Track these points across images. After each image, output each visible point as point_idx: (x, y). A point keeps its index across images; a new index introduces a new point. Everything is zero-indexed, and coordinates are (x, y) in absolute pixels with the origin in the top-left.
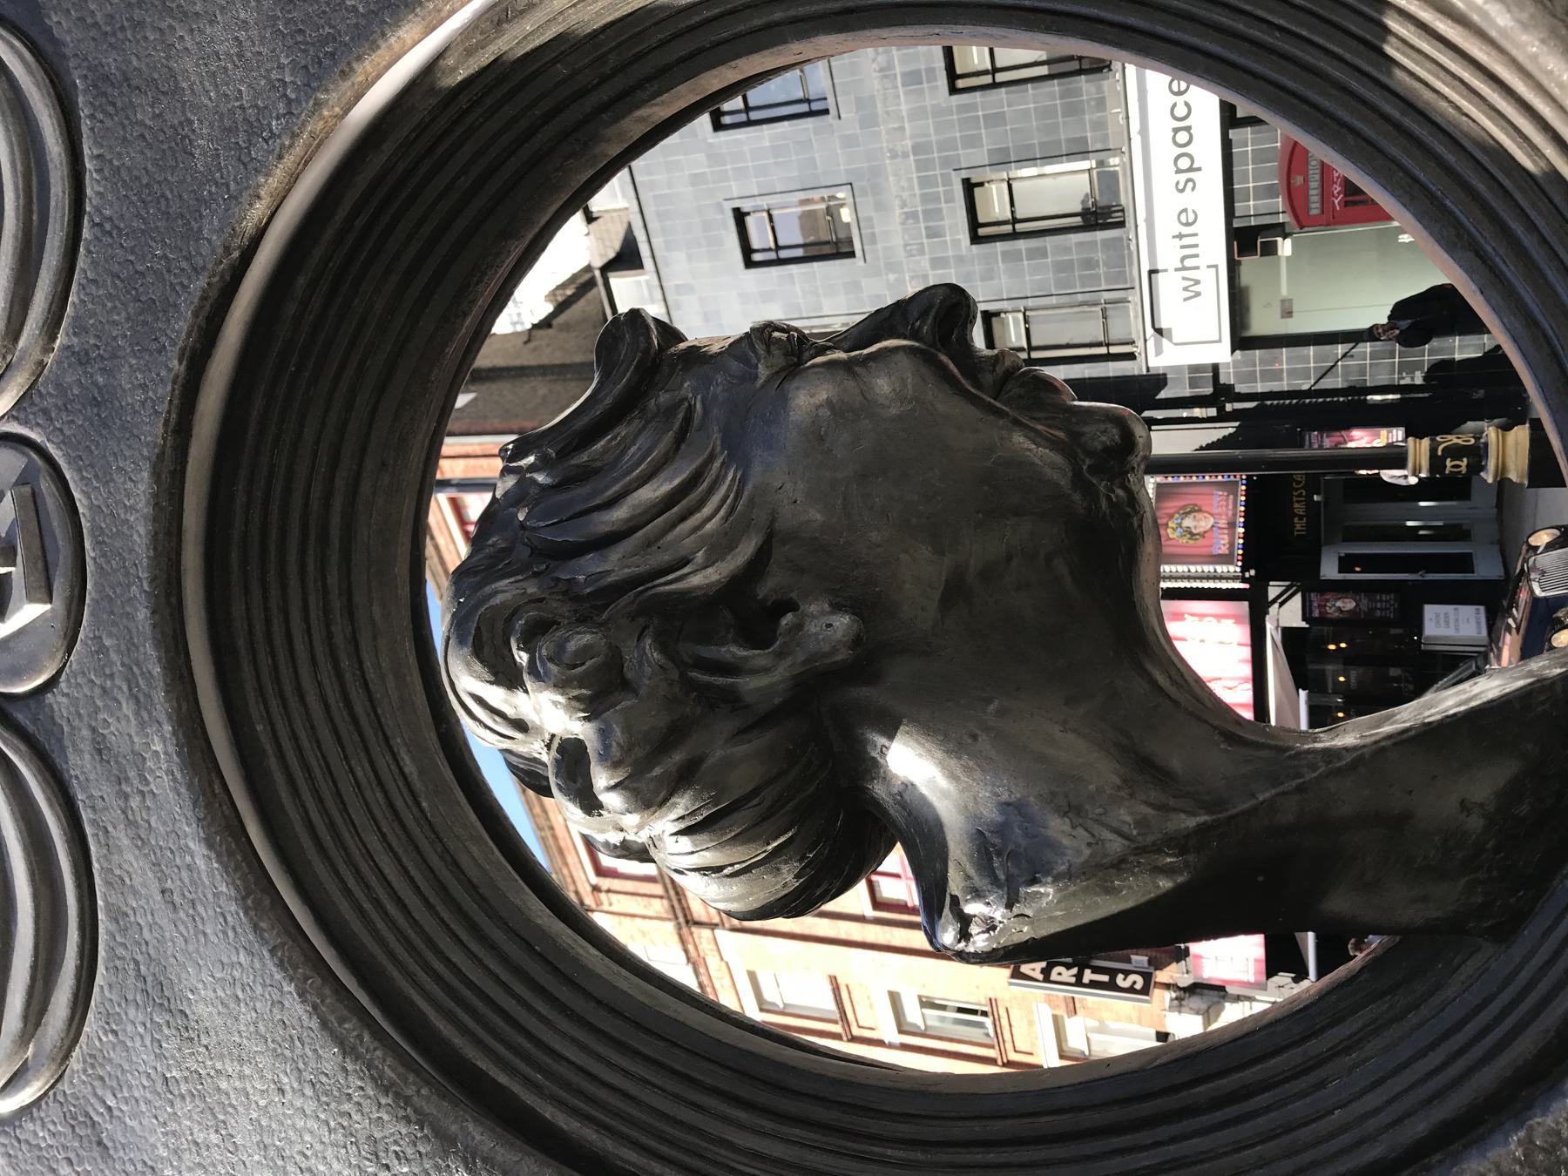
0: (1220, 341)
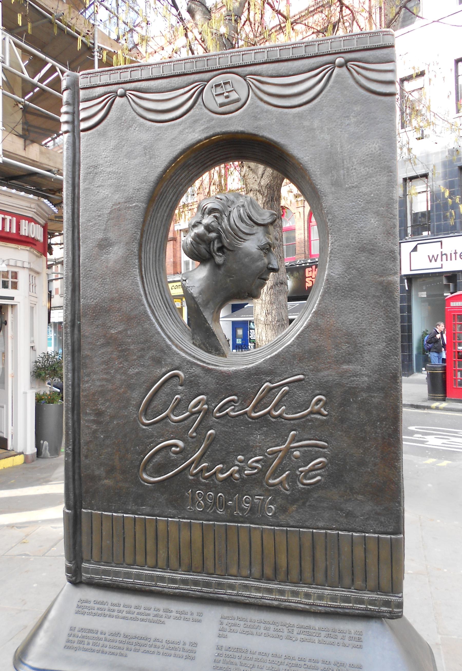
0: (411, 270)
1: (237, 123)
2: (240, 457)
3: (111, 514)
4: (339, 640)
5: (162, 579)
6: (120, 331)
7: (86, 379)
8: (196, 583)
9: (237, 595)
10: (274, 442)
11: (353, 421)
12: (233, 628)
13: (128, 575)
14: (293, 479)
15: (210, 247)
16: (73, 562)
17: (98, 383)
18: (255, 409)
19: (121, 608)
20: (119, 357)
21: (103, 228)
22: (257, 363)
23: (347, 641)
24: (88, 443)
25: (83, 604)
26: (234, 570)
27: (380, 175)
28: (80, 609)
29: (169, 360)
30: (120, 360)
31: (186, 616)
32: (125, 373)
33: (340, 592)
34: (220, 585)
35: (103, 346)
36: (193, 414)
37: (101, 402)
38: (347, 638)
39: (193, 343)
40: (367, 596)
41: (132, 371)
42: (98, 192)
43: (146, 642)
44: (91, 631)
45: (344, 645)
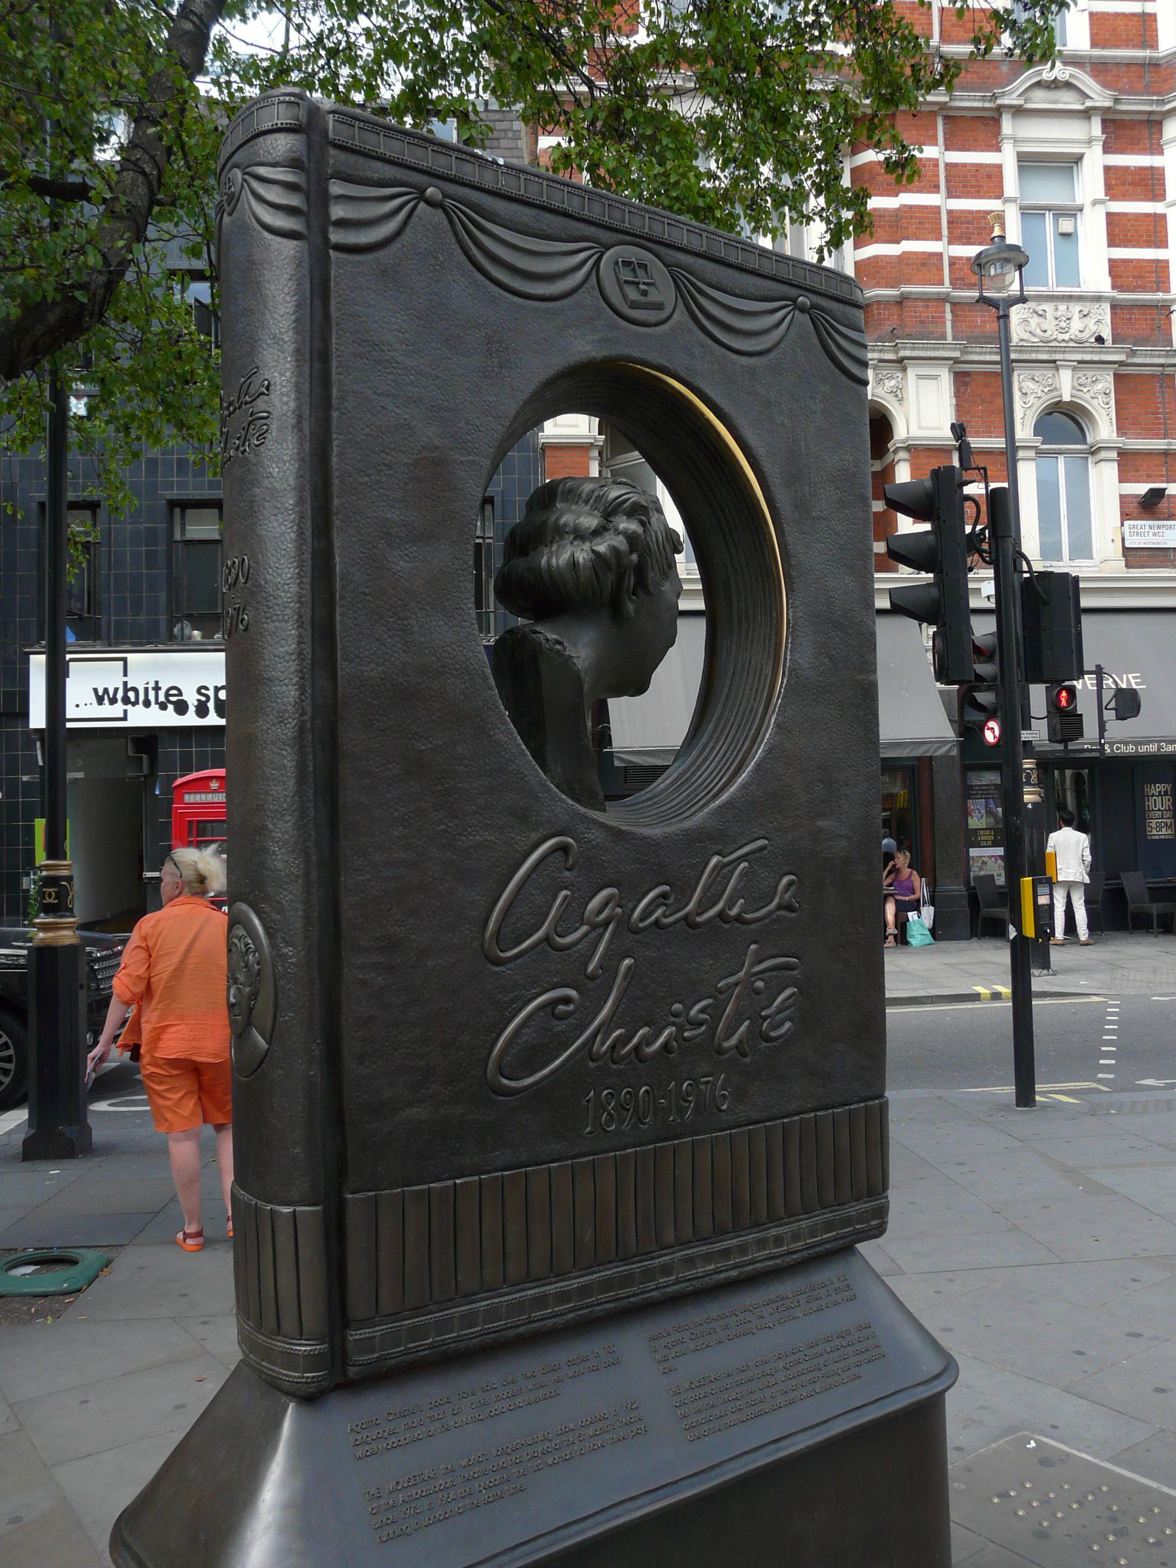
2: (677, 1007)
3: (425, 1187)
5: (540, 1302)
9: (677, 1282)
13: (469, 1320)
18: (703, 907)
33: (820, 1218)
34: (648, 1274)
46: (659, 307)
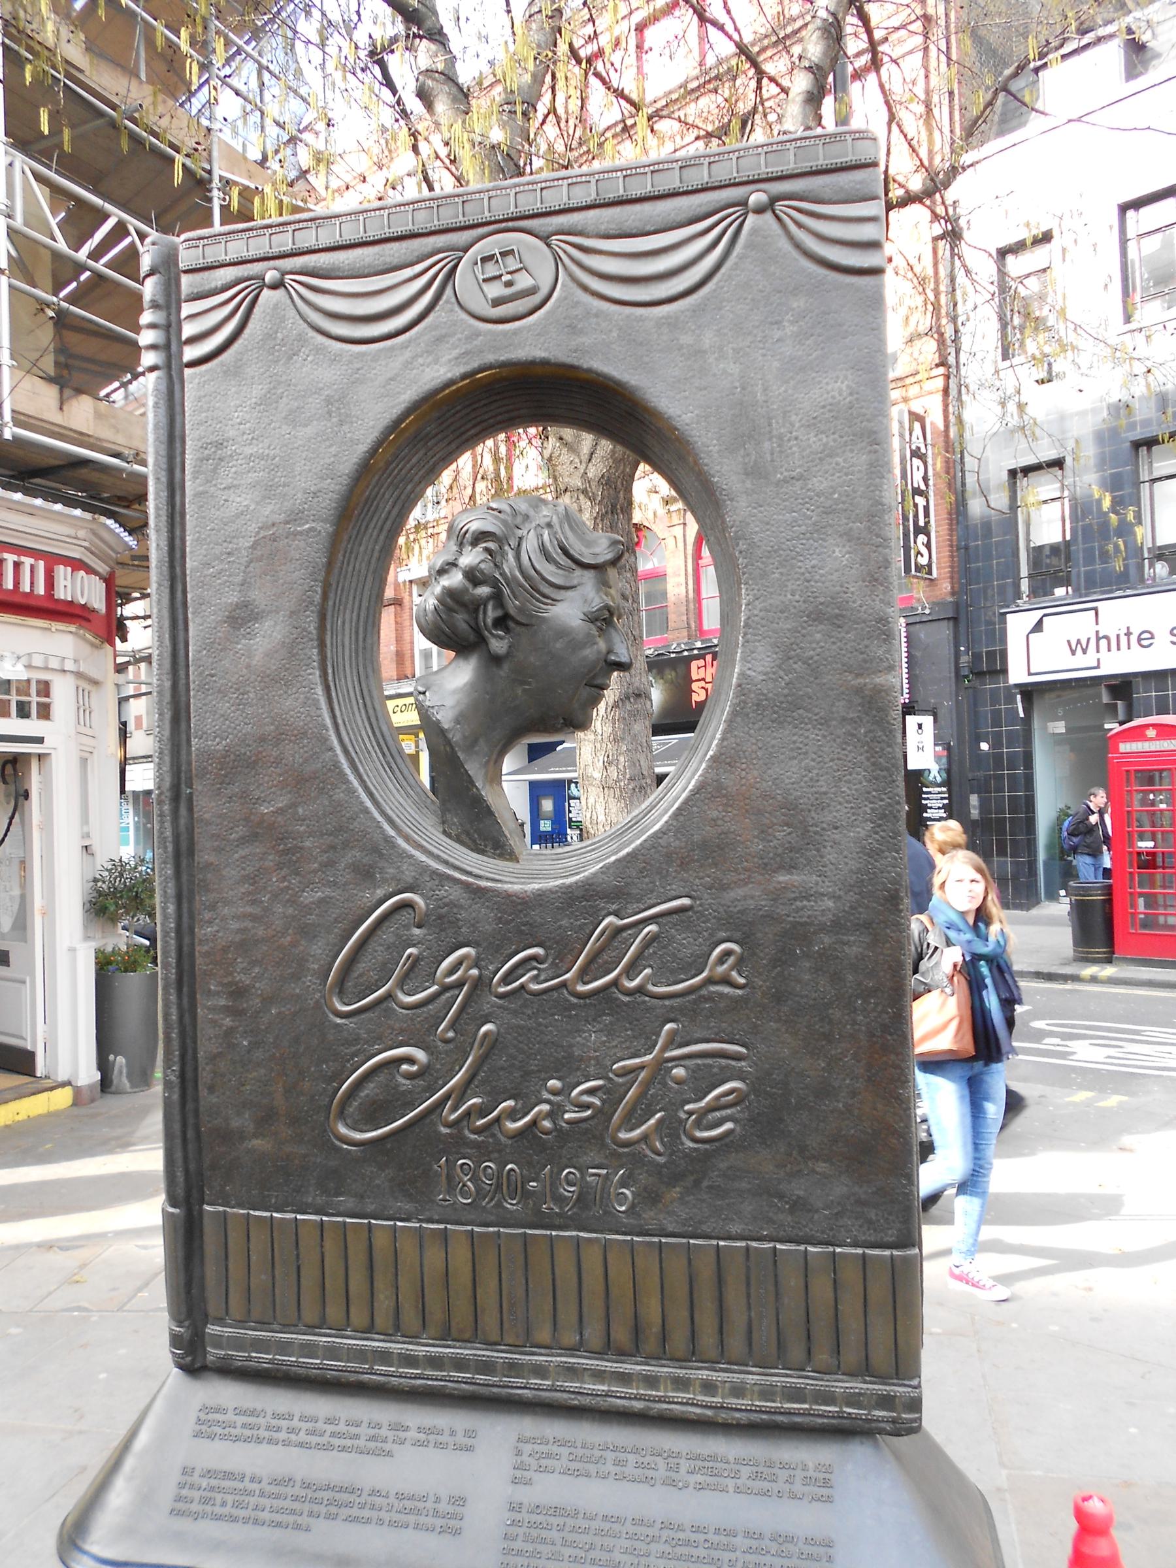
1: (531, 342)
2: (553, 1083)
3: (267, 1214)
4: (780, 1485)
5: (384, 1357)
6: (281, 809)
7: (207, 915)
8: (460, 1364)
9: (553, 1389)
10: (628, 1048)
11: (802, 997)
12: (544, 1462)
13: (309, 1350)
14: (671, 1129)
15: (476, 618)
16: (187, 1323)
17: (234, 925)
18: (585, 974)
19: (296, 1423)
20: (279, 866)
21: (239, 579)
22: (586, 874)
23: (798, 1487)
24: (213, 1058)
25: (210, 1416)
26: (544, 1334)
27: (852, 451)
28: (204, 1428)
29: (391, 871)
30: (283, 873)
31: (440, 1438)
32: (292, 902)
33: (781, 1379)
34: (513, 1368)
35: (243, 841)
36: (446, 988)
37: (241, 966)
38: (798, 1481)
39: (445, 832)
40: (842, 1385)
41: (308, 897)
42: (226, 500)
43: (352, 1498)
44: (228, 1475)
45: (793, 1496)
46: (532, 291)
